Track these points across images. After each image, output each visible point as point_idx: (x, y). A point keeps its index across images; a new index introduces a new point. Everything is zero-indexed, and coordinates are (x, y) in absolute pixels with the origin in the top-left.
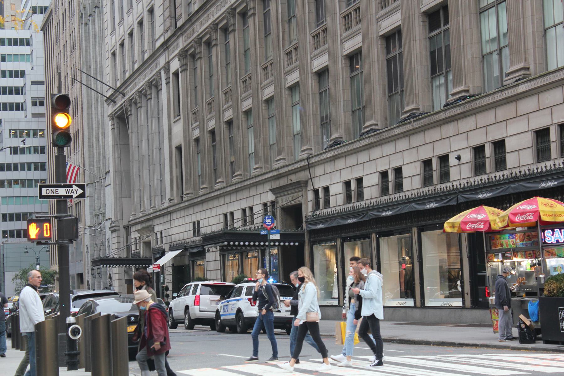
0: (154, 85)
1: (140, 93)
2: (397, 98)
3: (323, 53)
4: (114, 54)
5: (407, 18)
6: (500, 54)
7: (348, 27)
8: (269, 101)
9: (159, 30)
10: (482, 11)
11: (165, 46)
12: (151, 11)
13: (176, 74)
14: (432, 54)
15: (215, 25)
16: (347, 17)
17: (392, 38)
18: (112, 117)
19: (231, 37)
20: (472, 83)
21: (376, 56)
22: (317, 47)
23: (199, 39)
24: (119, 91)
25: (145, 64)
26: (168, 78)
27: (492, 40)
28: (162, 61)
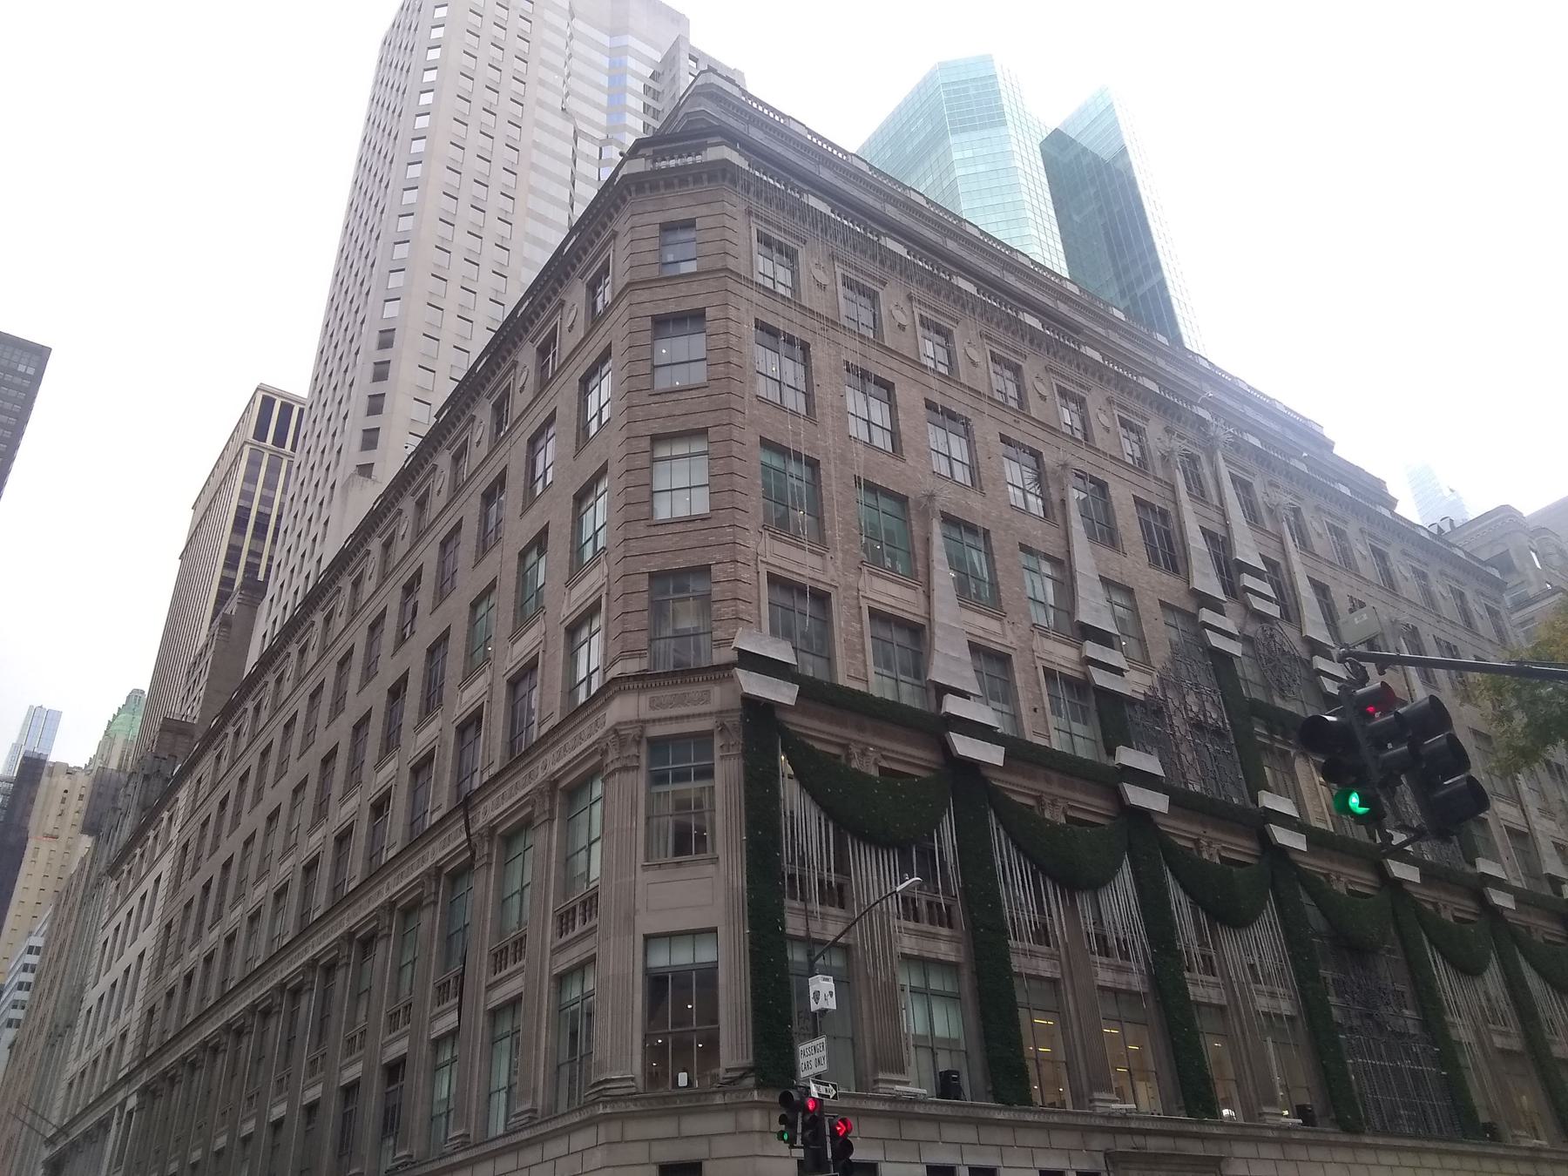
0: (104, 1125)
1: (87, 1135)
2: (346, 1159)
3: (283, 1100)
4: (71, 1084)
5: (367, 1071)
6: (447, 1117)
7: (312, 1073)
8: (219, 1153)
9: (126, 1059)
10: (437, 1069)
11: (128, 1078)
12: (124, 1036)
13: (130, 1113)
14: (386, 1111)
15: (184, 1059)
16: (313, 1062)
17: (351, 1090)
18: (47, 1164)
19: (197, 1073)
20: (416, 1148)
21: (333, 1108)
22: (279, 1092)
23: (165, 1072)
24: (63, 1131)
25: (102, 1098)
26: (120, 1117)
27: (441, 1102)
28: (120, 1096)
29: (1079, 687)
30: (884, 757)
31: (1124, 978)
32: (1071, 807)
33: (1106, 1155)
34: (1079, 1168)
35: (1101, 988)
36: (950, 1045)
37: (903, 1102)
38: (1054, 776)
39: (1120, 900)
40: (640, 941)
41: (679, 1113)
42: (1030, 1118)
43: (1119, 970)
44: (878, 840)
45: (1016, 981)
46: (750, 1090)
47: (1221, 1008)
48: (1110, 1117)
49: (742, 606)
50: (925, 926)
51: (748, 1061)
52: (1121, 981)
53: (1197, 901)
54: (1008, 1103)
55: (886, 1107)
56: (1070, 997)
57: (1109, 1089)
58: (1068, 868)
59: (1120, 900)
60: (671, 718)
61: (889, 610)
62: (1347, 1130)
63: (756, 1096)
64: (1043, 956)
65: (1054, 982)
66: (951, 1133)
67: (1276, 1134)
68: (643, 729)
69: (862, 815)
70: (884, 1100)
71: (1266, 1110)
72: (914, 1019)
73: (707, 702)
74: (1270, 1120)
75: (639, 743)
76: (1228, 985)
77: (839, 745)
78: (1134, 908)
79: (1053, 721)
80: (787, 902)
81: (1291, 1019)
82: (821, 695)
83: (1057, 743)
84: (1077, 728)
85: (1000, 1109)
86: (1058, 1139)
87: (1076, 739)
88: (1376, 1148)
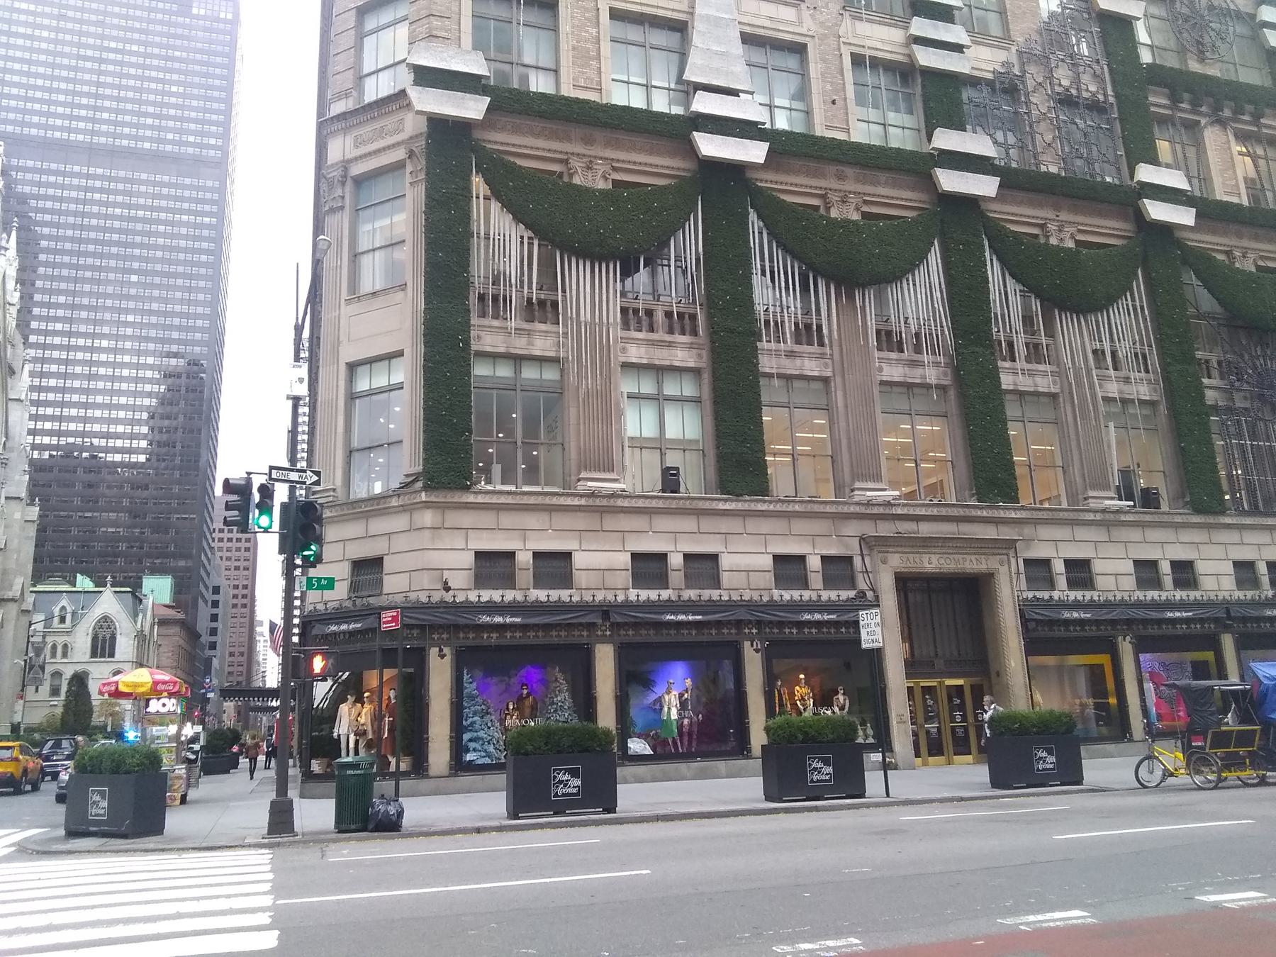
29: (905, 72)
30: (614, 169)
31: (918, 371)
32: (865, 202)
33: (863, 539)
34: (825, 552)
35: (882, 383)
36: (683, 446)
37: (603, 497)
38: (849, 171)
39: (920, 298)
40: (343, 368)
41: (367, 516)
42: (761, 507)
43: (913, 364)
44: (592, 252)
45: (763, 381)
46: (420, 491)
47: (1054, 396)
48: (869, 504)
49: (436, 22)
50: (660, 335)
51: (420, 468)
52: (915, 376)
53: (1030, 286)
54: (737, 494)
55: (583, 502)
56: (840, 394)
57: (878, 478)
58: (847, 263)
59: (920, 298)
60: (370, 154)
61: (668, 14)
62: (1198, 511)
63: (423, 497)
64: (811, 356)
65: (825, 380)
66: (663, 523)
67: (1099, 517)
68: (346, 169)
69: (574, 228)
70: (582, 496)
71: (1091, 493)
72: (637, 423)
73: (403, 130)
74: (1093, 504)
75: (343, 183)
76: (1060, 374)
77: (561, 161)
78: (938, 304)
79: (855, 111)
80: (475, 320)
81: (1152, 404)
82: (511, 103)
83: (861, 134)
84: (892, 117)
85: (726, 500)
86: (799, 526)
87: (891, 130)
88: (1240, 528)
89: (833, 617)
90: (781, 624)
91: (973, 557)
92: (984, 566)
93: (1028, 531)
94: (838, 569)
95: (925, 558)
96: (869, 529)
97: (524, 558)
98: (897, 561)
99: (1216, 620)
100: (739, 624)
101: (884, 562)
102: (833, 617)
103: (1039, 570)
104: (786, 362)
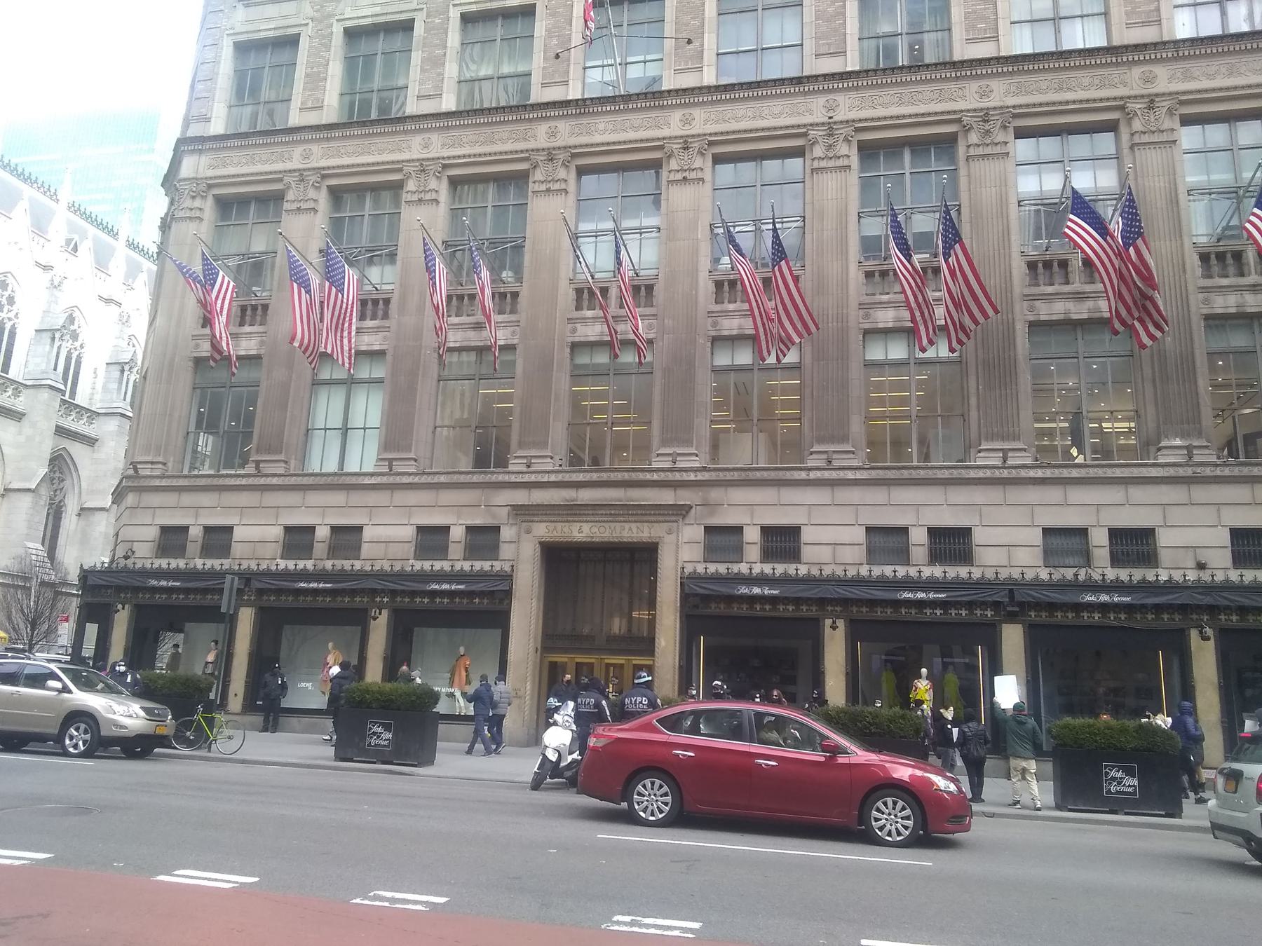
34: (470, 522)
89: (462, 587)
90: (413, 594)
91: (634, 526)
92: (646, 534)
93: (715, 494)
94: (483, 539)
95: (575, 528)
96: (521, 497)
97: (195, 532)
98: (544, 530)
99: (996, 605)
100: (374, 592)
101: (528, 532)
102: (462, 587)
103: (723, 539)
104: (471, 334)
